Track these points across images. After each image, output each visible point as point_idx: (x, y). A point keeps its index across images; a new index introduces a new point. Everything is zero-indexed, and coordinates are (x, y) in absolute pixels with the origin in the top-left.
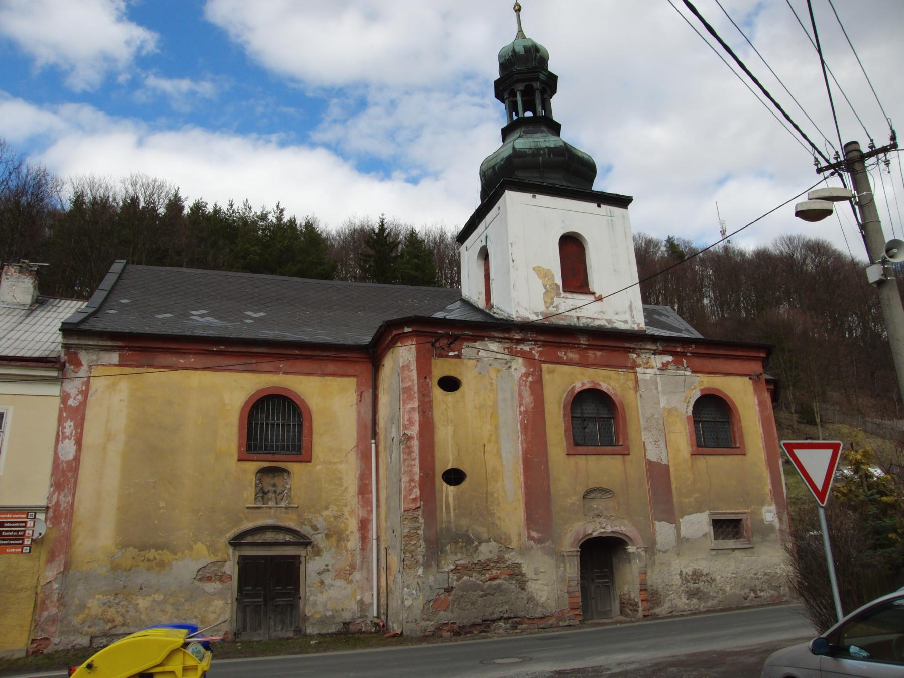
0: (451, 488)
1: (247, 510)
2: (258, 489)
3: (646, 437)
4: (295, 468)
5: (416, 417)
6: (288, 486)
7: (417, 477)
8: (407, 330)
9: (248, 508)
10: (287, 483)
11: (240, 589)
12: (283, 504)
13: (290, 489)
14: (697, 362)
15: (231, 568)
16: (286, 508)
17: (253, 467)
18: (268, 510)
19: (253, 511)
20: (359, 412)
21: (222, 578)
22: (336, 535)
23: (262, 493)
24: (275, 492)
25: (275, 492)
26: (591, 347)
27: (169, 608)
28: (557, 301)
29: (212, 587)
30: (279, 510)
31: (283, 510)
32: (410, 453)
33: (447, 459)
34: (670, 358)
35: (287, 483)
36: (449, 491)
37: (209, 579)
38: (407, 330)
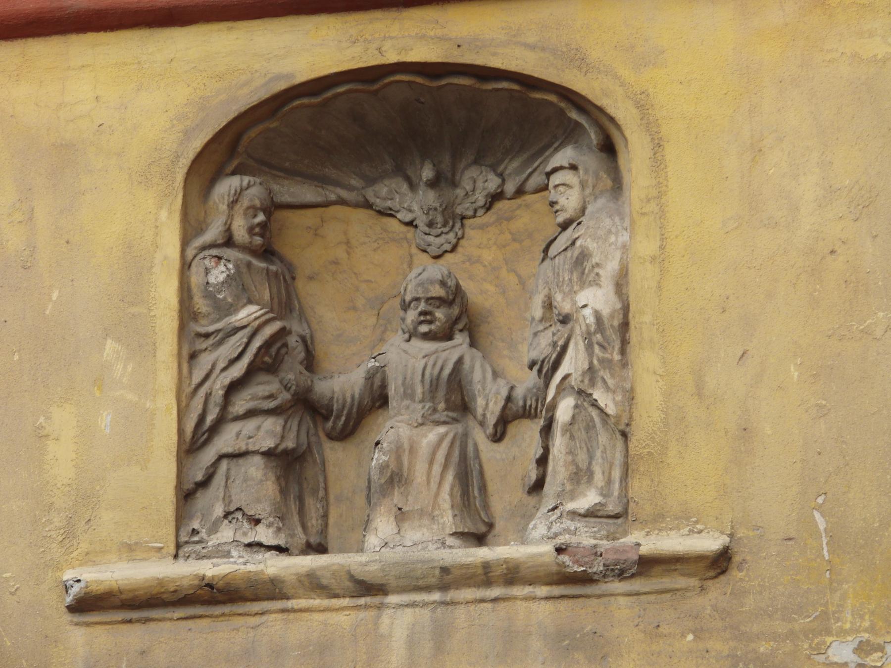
1: (82, 638)
2: (223, 362)
6: (594, 300)
9: (88, 605)
10: (582, 267)
12: (532, 546)
13: (619, 332)
16: (572, 579)
18: (344, 618)
19: (167, 635)
23: (281, 419)
24: (453, 396)
25: (453, 396)
30: (473, 617)
31: (536, 610)
35: (582, 267)
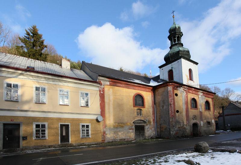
0: (177, 114)
3: (200, 107)
4: (142, 109)
5: (172, 100)
7: (173, 111)
8: (170, 84)
11: (135, 131)
14: (206, 95)
15: (134, 127)
17: (136, 108)
20: (152, 99)
21: (132, 129)
22: (149, 122)
26: (194, 90)
27: (124, 135)
28: (189, 81)
29: (131, 131)
32: (171, 107)
33: (177, 109)
34: (202, 94)
36: (177, 114)
37: (130, 129)
38: (170, 84)
